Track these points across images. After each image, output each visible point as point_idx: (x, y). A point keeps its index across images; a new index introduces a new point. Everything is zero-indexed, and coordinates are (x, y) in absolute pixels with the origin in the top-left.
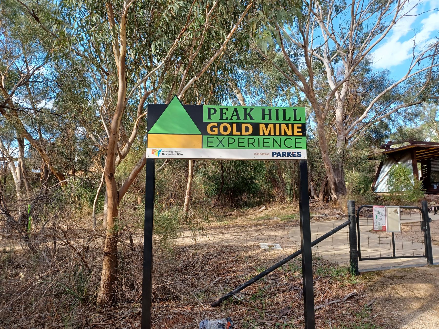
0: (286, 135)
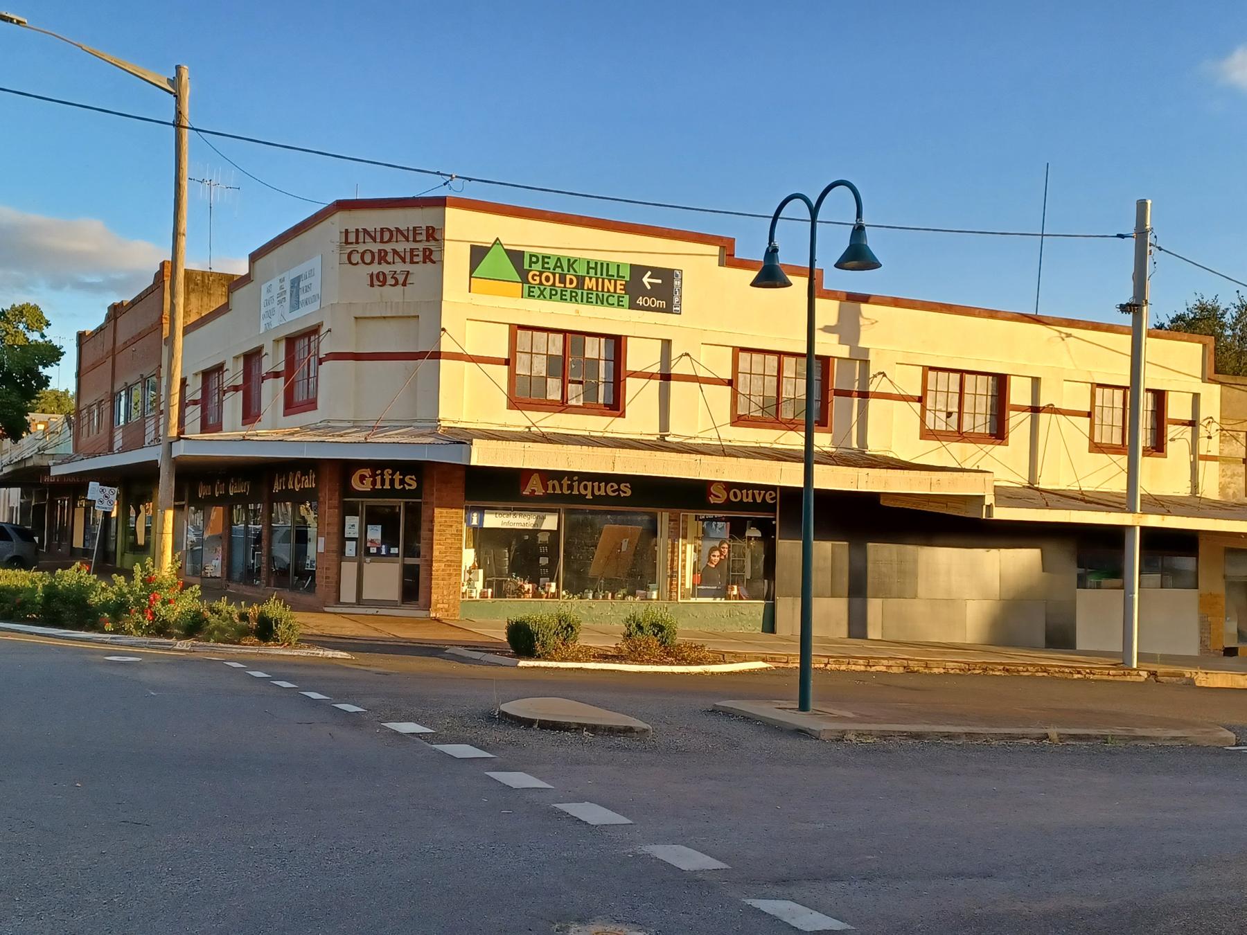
0: (609, 291)
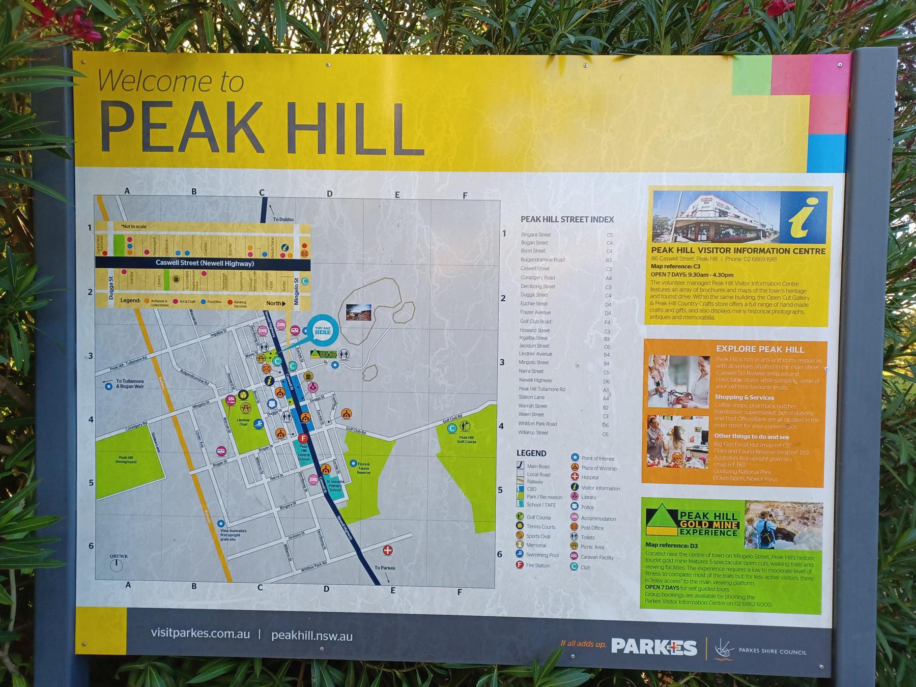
0: (728, 528)
